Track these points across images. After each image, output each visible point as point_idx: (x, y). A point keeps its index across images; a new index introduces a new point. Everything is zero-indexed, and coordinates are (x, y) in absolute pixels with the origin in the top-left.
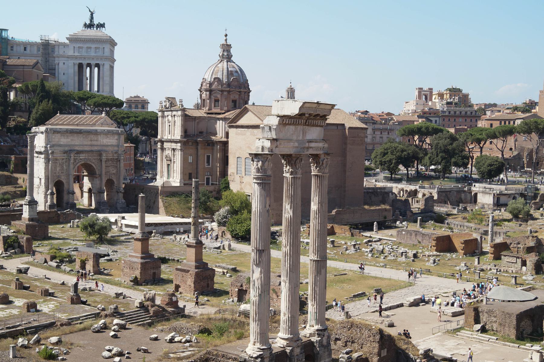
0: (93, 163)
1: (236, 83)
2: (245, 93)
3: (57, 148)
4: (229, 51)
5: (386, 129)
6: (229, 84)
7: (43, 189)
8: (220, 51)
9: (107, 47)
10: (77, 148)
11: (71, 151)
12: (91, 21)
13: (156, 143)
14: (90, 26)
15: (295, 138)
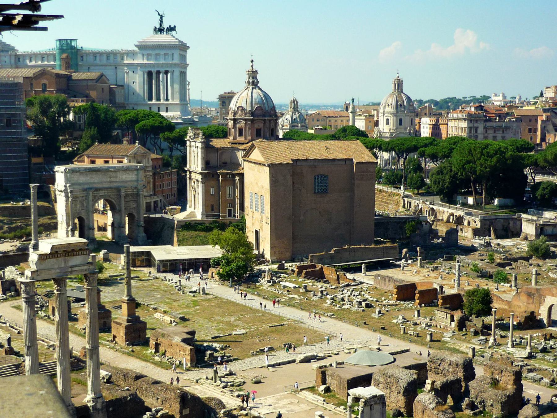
0: (113, 199)
1: (260, 112)
2: (270, 121)
3: (76, 187)
4: (255, 77)
5: (500, 127)
6: (252, 114)
7: (65, 225)
8: (246, 78)
9: (177, 53)
10: (95, 186)
11: (91, 188)
12: (161, 25)
13: (186, 172)
14: (160, 30)
15: (56, 266)
